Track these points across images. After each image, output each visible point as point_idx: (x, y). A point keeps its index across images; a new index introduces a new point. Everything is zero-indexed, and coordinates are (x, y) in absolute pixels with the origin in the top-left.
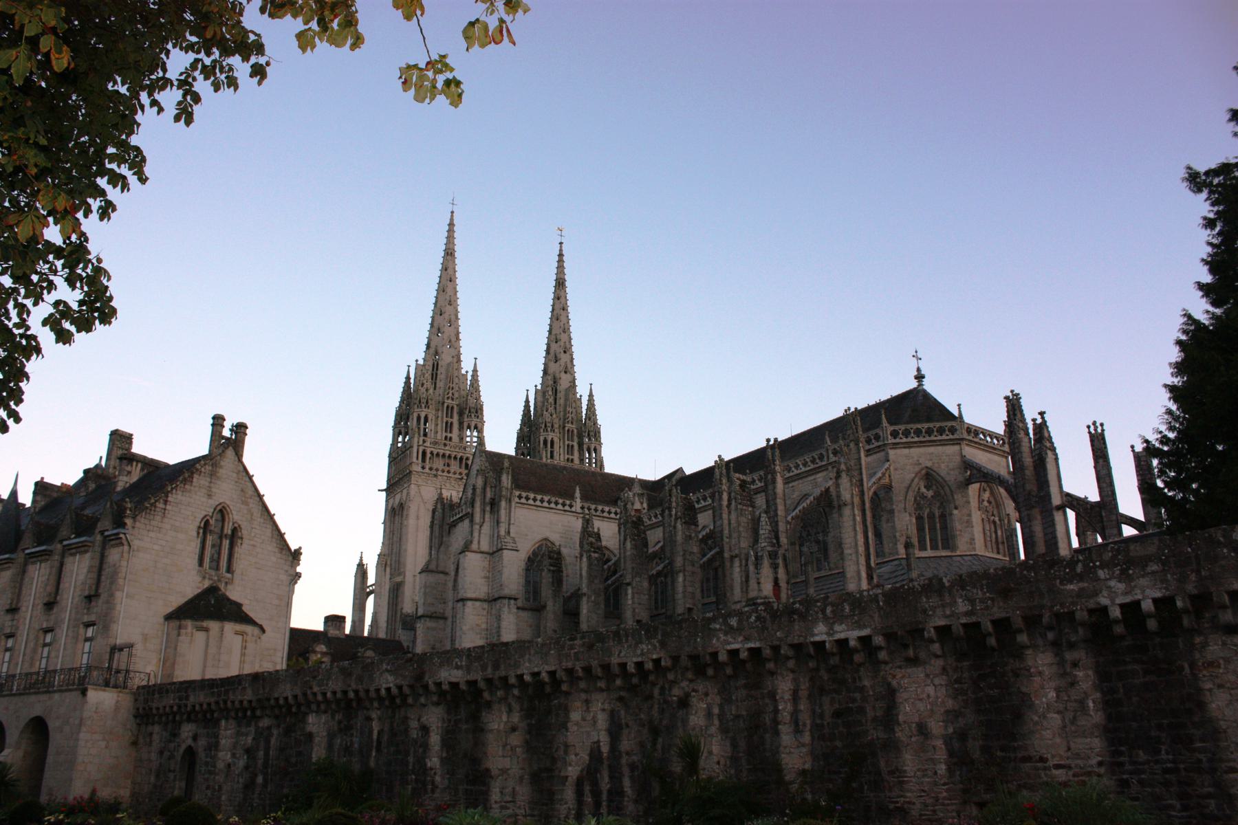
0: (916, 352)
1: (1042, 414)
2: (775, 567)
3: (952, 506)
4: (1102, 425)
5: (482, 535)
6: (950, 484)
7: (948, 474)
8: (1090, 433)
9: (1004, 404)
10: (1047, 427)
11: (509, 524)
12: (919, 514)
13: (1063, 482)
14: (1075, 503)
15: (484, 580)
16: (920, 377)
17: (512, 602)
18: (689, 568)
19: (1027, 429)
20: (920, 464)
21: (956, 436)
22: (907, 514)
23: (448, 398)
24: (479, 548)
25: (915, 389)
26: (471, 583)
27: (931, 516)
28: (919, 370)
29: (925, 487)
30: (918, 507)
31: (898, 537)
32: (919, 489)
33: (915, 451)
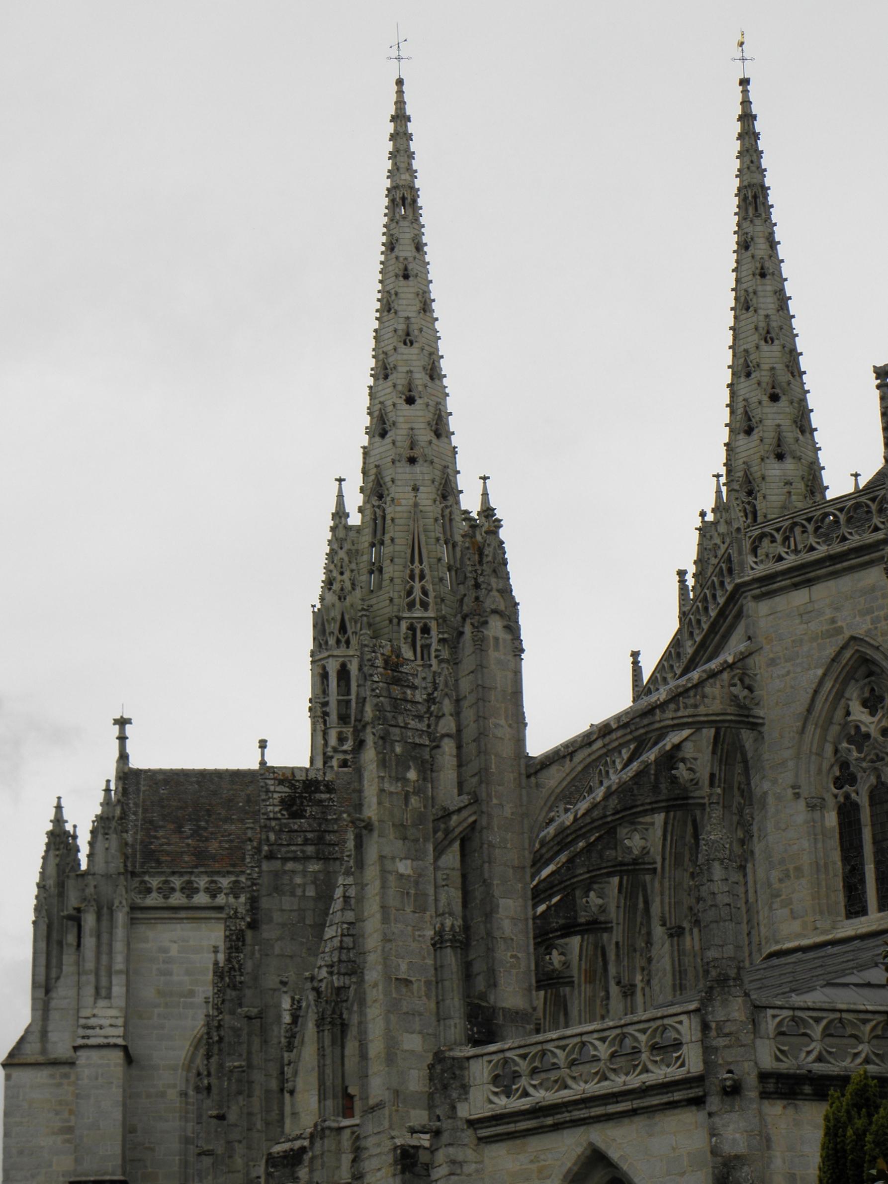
5: (54, 1015)
11: (110, 976)
12: (847, 796)
15: (59, 1139)
20: (839, 631)
22: (801, 805)
24: (44, 1051)
29: (865, 704)
32: (848, 714)
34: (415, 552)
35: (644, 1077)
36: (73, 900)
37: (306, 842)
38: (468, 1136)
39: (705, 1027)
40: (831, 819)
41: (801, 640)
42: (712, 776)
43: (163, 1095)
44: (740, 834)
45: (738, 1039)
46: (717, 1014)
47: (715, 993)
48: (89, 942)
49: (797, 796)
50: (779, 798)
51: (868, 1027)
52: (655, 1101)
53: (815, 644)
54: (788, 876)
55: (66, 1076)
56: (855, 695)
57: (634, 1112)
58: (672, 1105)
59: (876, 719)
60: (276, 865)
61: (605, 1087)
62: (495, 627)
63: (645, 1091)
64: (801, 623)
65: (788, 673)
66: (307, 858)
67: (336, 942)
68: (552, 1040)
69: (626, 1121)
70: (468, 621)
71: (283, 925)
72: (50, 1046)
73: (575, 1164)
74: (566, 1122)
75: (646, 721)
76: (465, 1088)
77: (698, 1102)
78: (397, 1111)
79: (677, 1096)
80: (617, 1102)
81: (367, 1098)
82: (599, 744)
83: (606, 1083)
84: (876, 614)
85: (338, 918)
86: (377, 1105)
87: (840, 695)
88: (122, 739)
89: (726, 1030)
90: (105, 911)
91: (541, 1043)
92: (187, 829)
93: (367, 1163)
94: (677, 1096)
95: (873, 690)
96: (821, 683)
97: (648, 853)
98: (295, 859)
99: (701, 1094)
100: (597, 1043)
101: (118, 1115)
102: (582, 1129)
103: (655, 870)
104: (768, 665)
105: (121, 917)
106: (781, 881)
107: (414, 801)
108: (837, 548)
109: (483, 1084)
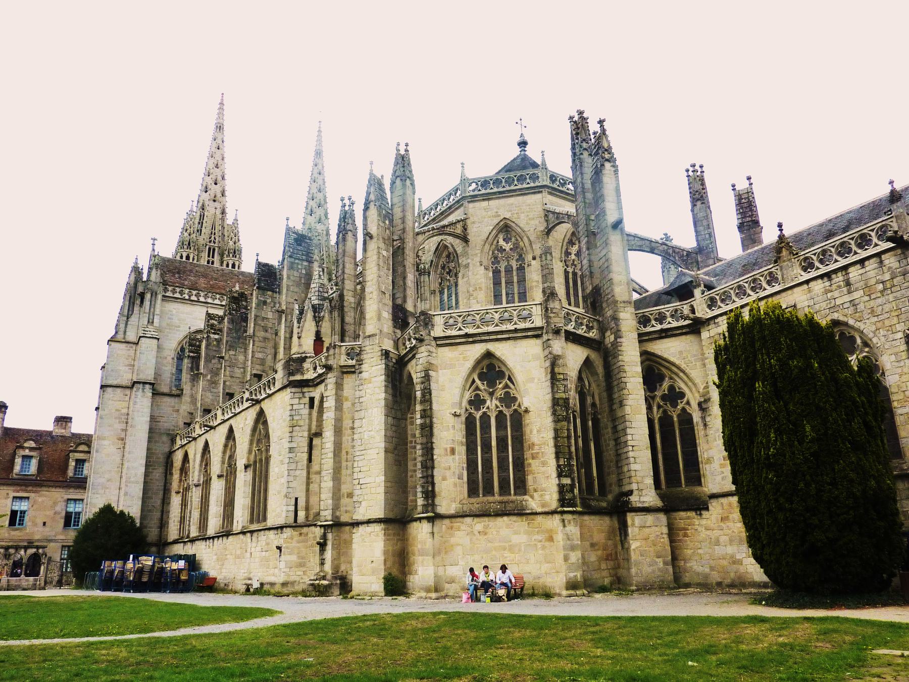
2: (318, 320)
3: (530, 257)
4: (701, 167)
5: (129, 326)
7: (528, 224)
8: (688, 176)
10: (606, 137)
11: (154, 316)
12: (496, 267)
13: (622, 197)
14: (671, 251)
16: (523, 144)
17: (147, 386)
18: (261, 334)
20: (499, 216)
21: (537, 184)
23: (210, 242)
24: (124, 338)
26: (112, 370)
27: (509, 270)
28: (522, 135)
29: (504, 240)
30: (496, 260)
32: (498, 242)
33: (493, 203)
34: (213, 227)
35: (515, 326)
36: (140, 289)
37: (303, 255)
38: (433, 343)
39: (547, 309)
40: (491, 274)
42: (432, 261)
43: (166, 358)
44: (440, 280)
46: (551, 305)
48: (147, 303)
49: (481, 265)
50: (474, 265)
51: (585, 321)
55: (132, 347)
57: (509, 339)
60: (292, 260)
61: (497, 329)
63: (516, 330)
66: (303, 260)
67: (317, 289)
70: (398, 179)
71: (294, 281)
72: (126, 337)
76: (433, 325)
77: (537, 336)
79: (529, 334)
82: (431, 232)
85: (317, 281)
88: (153, 244)
90: (154, 294)
92: (177, 276)
94: (529, 334)
98: (299, 259)
101: (154, 361)
105: (160, 297)
107: (387, 231)
108: (501, 189)
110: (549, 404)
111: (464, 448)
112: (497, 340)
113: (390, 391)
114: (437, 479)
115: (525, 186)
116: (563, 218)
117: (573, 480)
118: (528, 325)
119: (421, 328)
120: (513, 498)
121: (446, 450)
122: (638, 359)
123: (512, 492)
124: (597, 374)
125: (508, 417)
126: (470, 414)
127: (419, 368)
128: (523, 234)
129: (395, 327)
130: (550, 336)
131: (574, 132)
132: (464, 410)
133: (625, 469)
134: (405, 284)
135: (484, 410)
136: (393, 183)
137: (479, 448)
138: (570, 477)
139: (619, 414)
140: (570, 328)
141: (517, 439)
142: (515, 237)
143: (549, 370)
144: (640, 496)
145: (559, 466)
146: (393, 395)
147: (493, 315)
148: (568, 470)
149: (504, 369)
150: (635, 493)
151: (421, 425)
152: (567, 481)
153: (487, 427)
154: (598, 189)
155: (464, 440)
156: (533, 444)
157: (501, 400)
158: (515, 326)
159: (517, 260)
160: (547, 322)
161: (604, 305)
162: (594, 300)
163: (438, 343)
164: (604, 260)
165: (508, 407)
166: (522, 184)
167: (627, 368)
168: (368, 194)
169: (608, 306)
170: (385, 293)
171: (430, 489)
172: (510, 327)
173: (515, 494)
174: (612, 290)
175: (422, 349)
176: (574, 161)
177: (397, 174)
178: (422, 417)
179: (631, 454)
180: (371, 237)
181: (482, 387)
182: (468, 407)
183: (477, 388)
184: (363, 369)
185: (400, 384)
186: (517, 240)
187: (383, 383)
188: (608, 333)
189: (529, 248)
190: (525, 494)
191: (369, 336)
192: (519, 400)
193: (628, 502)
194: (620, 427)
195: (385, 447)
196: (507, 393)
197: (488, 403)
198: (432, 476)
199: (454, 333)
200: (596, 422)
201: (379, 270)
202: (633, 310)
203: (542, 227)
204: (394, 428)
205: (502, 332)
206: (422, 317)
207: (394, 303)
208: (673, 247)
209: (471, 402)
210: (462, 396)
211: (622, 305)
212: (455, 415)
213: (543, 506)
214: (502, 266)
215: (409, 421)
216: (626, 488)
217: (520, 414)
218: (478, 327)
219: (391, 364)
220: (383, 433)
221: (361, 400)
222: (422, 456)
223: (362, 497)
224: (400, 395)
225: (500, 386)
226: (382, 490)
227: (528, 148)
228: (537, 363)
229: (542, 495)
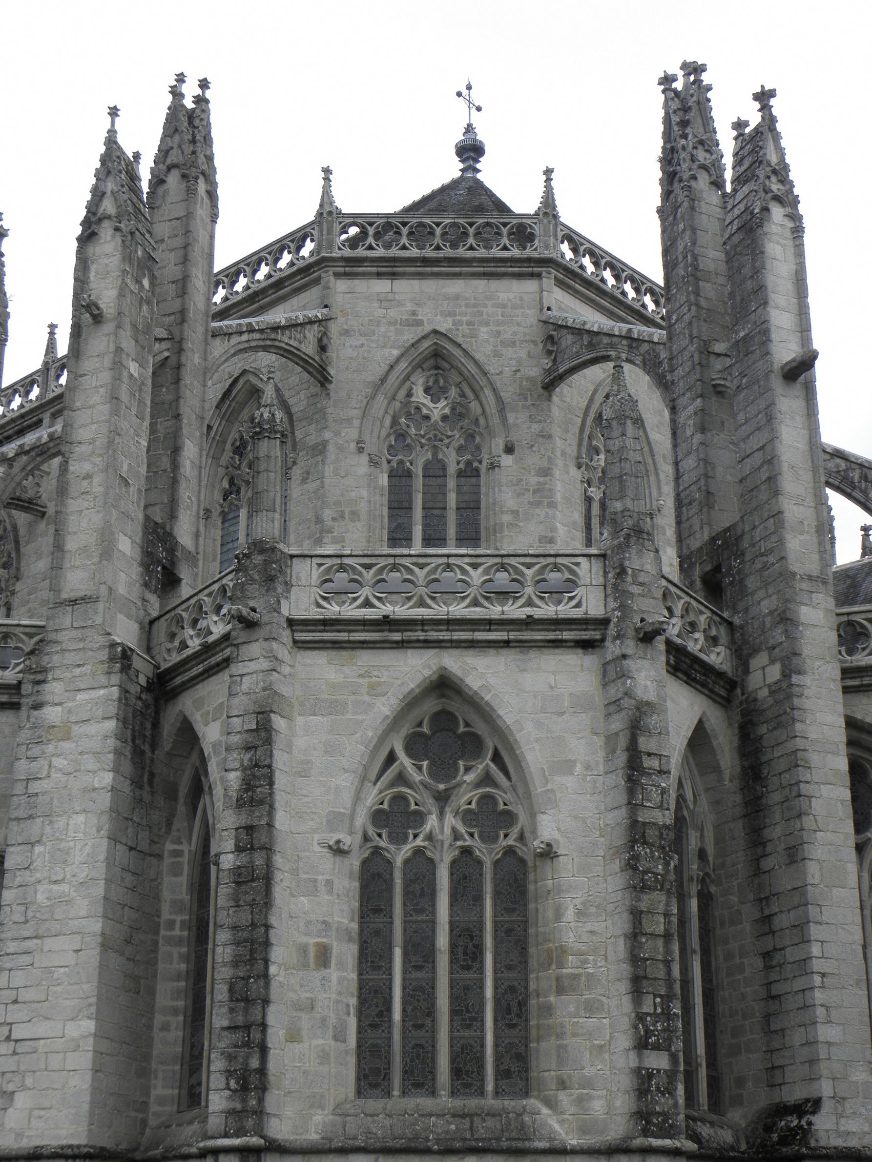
0: (469, 88)
1: (764, 97)
3: (498, 444)
6: (498, 384)
7: (497, 354)
9: (658, 98)
13: (811, 300)
14: (856, 475)
19: (721, 169)
20: (419, 323)
21: (529, 252)
22: (364, 459)
25: (454, 184)
28: (469, 129)
29: (427, 390)
31: (329, 523)
32: (409, 395)
33: (406, 288)
35: (529, 611)
38: (286, 635)
40: (384, 480)
41: (379, 322)
44: (226, 484)
45: (650, 591)
47: (633, 540)
49: (361, 450)
50: (340, 449)
51: (703, 618)
52: (539, 636)
53: (392, 328)
54: (342, 517)
56: (421, 381)
57: (507, 644)
58: (556, 644)
59: (440, 405)
61: (476, 613)
62: (202, 187)
63: (529, 623)
64: (380, 308)
65: (362, 345)
68: (410, 556)
69: (492, 651)
73: (418, 686)
74: (418, 641)
75: (273, 336)
76: (288, 586)
77: (586, 645)
78: (109, 609)
79: (567, 635)
80: (489, 630)
81: (59, 591)
82: (245, 337)
83: (478, 609)
84: (458, 318)
86: (82, 599)
87: (407, 378)
89: (641, 580)
91: (395, 556)
93: (55, 657)
94: (567, 635)
95: (436, 381)
96: (398, 360)
97: (39, 497)
99: (598, 637)
100: (468, 568)
102: (432, 652)
103: (44, 513)
104: (341, 335)
106: (334, 519)
108: (429, 253)
109: (310, 586)
110: (619, 838)
111: (354, 948)
112: (472, 644)
113: (127, 767)
114: (276, 1036)
115: (496, 252)
116: (612, 346)
117: (674, 1058)
118: (565, 610)
119: (252, 589)
120: (490, 1102)
121: (303, 950)
122: (840, 736)
123: (490, 1087)
124: (717, 769)
125: (488, 868)
126: (377, 851)
127: (240, 703)
128: (483, 382)
129: (146, 585)
130: (630, 646)
131: (676, 119)
132: (359, 837)
133: (796, 1037)
134: (175, 466)
135: (419, 842)
136: (157, 181)
137: (398, 953)
138: (668, 1049)
139: (784, 881)
140: (674, 629)
141: (508, 932)
142: (458, 385)
143: (623, 741)
144: (840, 1116)
145: (640, 1018)
146: (133, 782)
147: (464, 571)
148: (664, 1030)
149: (480, 728)
150: (827, 1106)
151: (237, 871)
152: (658, 1061)
153: (422, 894)
154: (747, 271)
155: (355, 926)
156: (563, 951)
157: (468, 817)
158: (529, 611)
159: (460, 450)
160: (622, 607)
161: (751, 583)
162: (717, 569)
163: (301, 636)
164: (758, 459)
165: (489, 838)
166: (488, 247)
167: (814, 758)
168: (98, 194)
169: (766, 585)
170: (127, 484)
171: (255, 1063)
172: (515, 611)
173: (497, 1093)
174: (781, 542)
175: (255, 649)
176: (667, 195)
177: (173, 158)
178: (239, 849)
179: (819, 996)
180: (98, 318)
181: (417, 777)
182: (371, 831)
183: (401, 779)
184: (48, 698)
185: (153, 749)
186: (463, 395)
187: (111, 742)
188: (759, 660)
189: (495, 420)
190: (526, 1094)
191: (73, 602)
192: (523, 818)
193: (805, 1132)
194: (783, 921)
195: (103, 934)
196: (487, 800)
197: (432, 822)
198: (264, 1026)
199: (350, 611)
200: (705, 899)
201: (116, 412)
202: (830, 603)
203: (535, 371)
204: (129, 879)
205: (490, 624)
206: (258, 559)
207: (147, 518)
208: (861, 465)
209: (378, 817)
210: (357, 798)
211: (805, 585)
212: (338, 850)
213: (584, 1130)
214: (419, 461)
215: (167, 861)
216: (794, 1094)
217: (522, 861)
218: (422, 604)
219: (134, 689)
220: (99, 889)
221: (34, 787)
222: (235, 964)
223: (17, 1079)
224: (151, 784)
225: (470, 778)
226: (83, 1060)
227: (483, 164)
228: (584, 719)
229: (580, 1100)
